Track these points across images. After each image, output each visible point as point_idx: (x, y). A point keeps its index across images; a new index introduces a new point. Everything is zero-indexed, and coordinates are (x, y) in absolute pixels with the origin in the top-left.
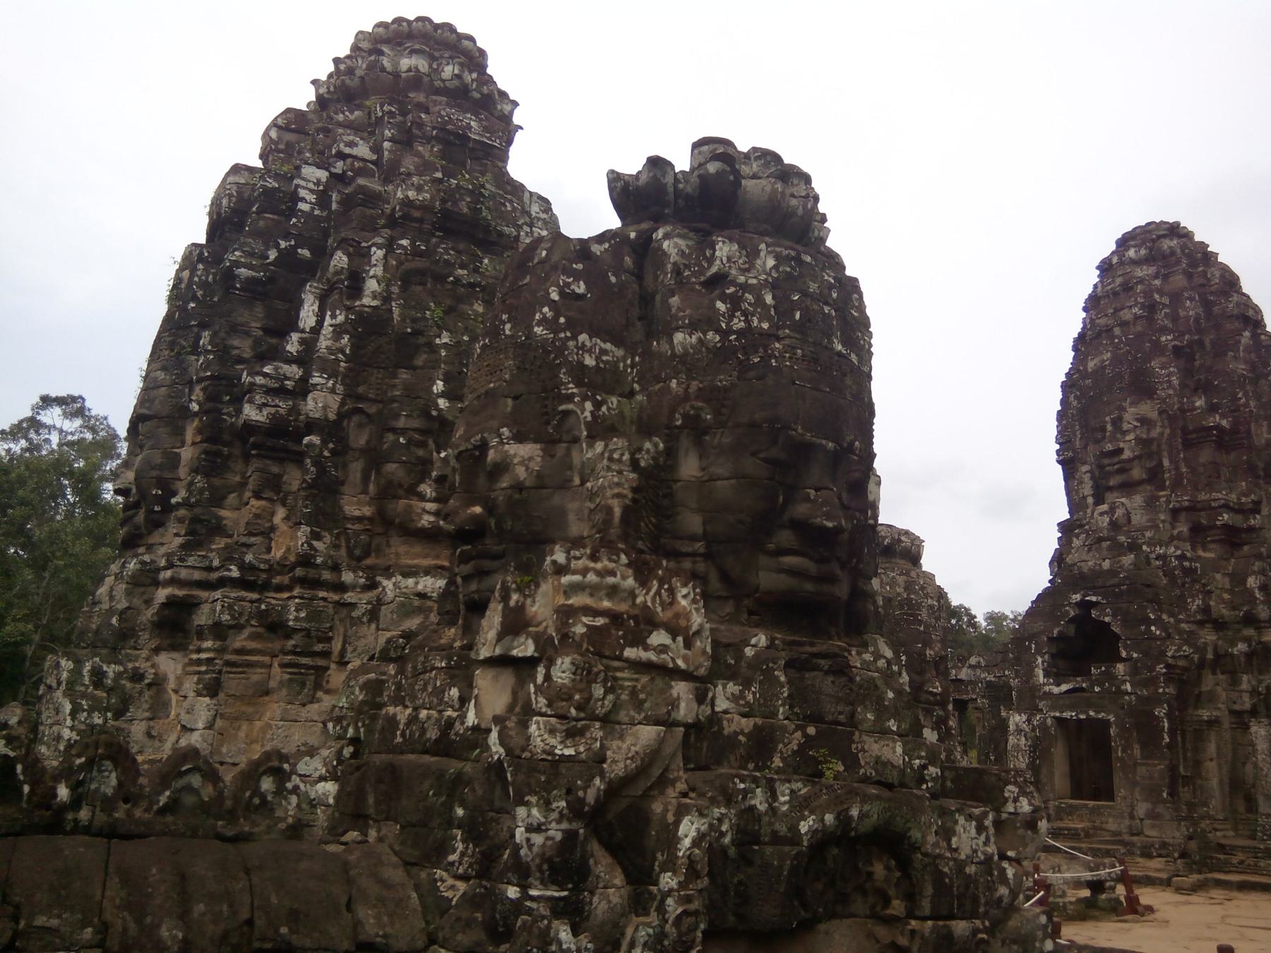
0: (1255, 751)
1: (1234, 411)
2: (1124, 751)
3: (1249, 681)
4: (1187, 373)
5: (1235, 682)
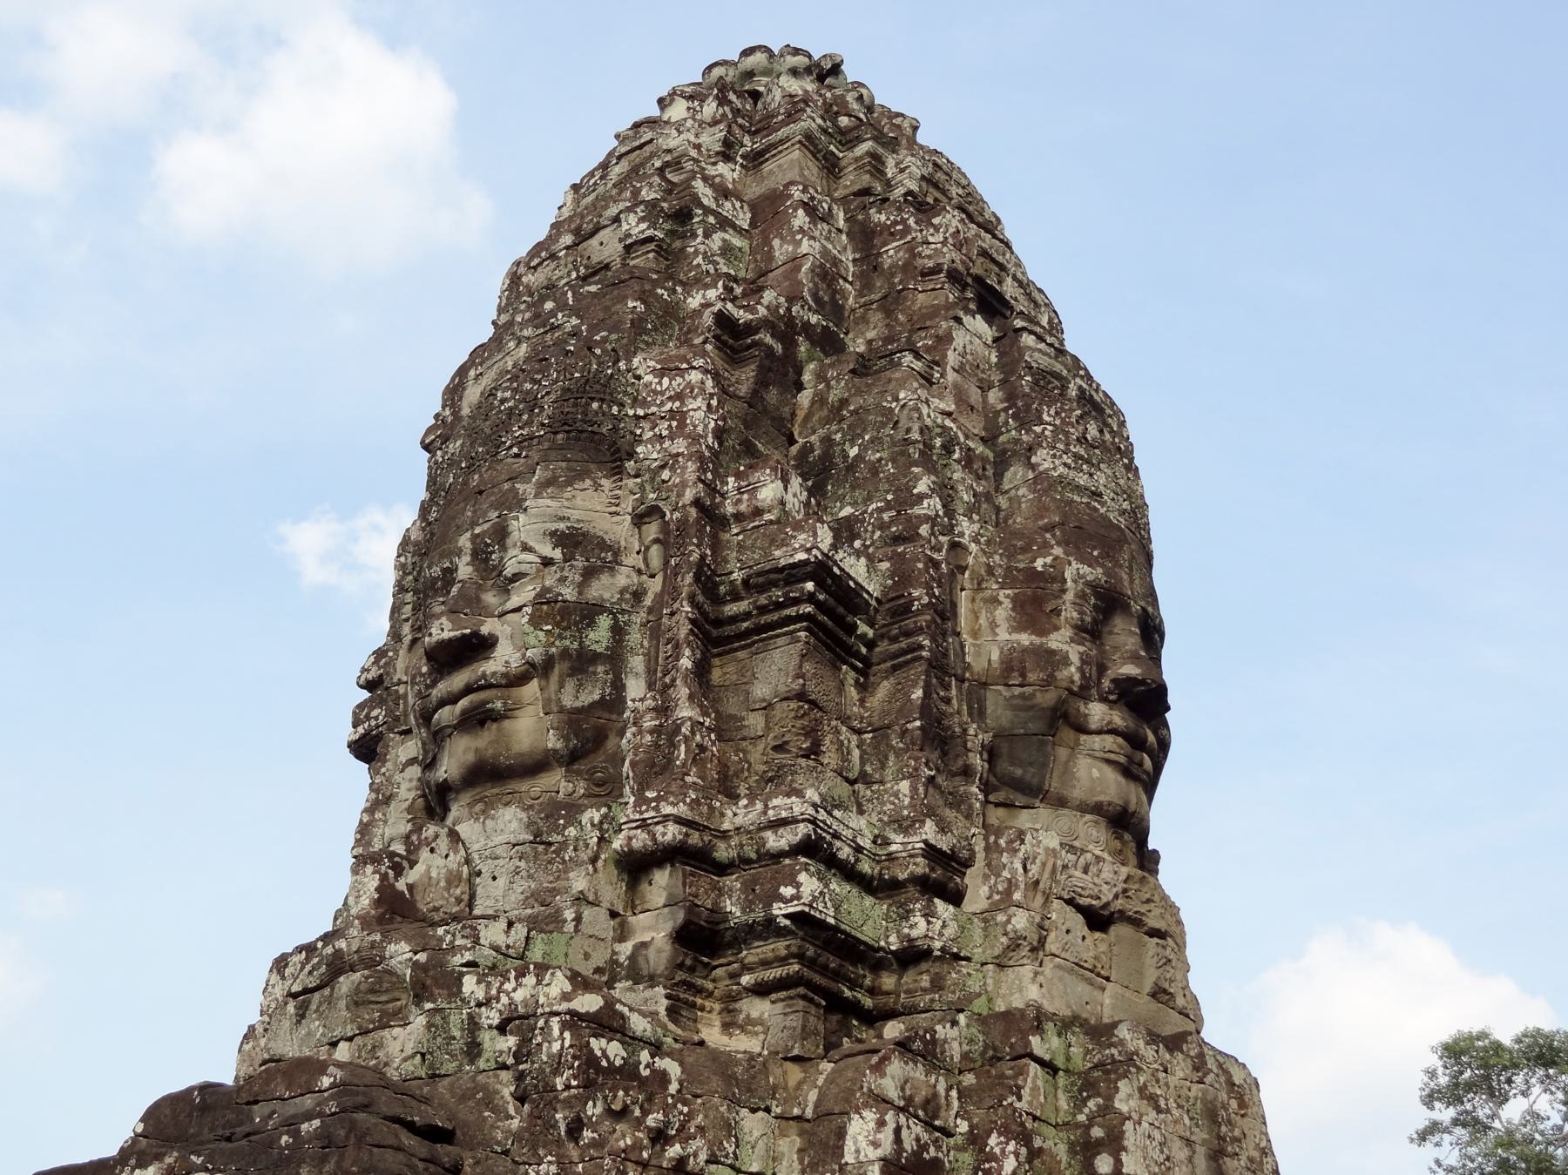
1: (897, 539)
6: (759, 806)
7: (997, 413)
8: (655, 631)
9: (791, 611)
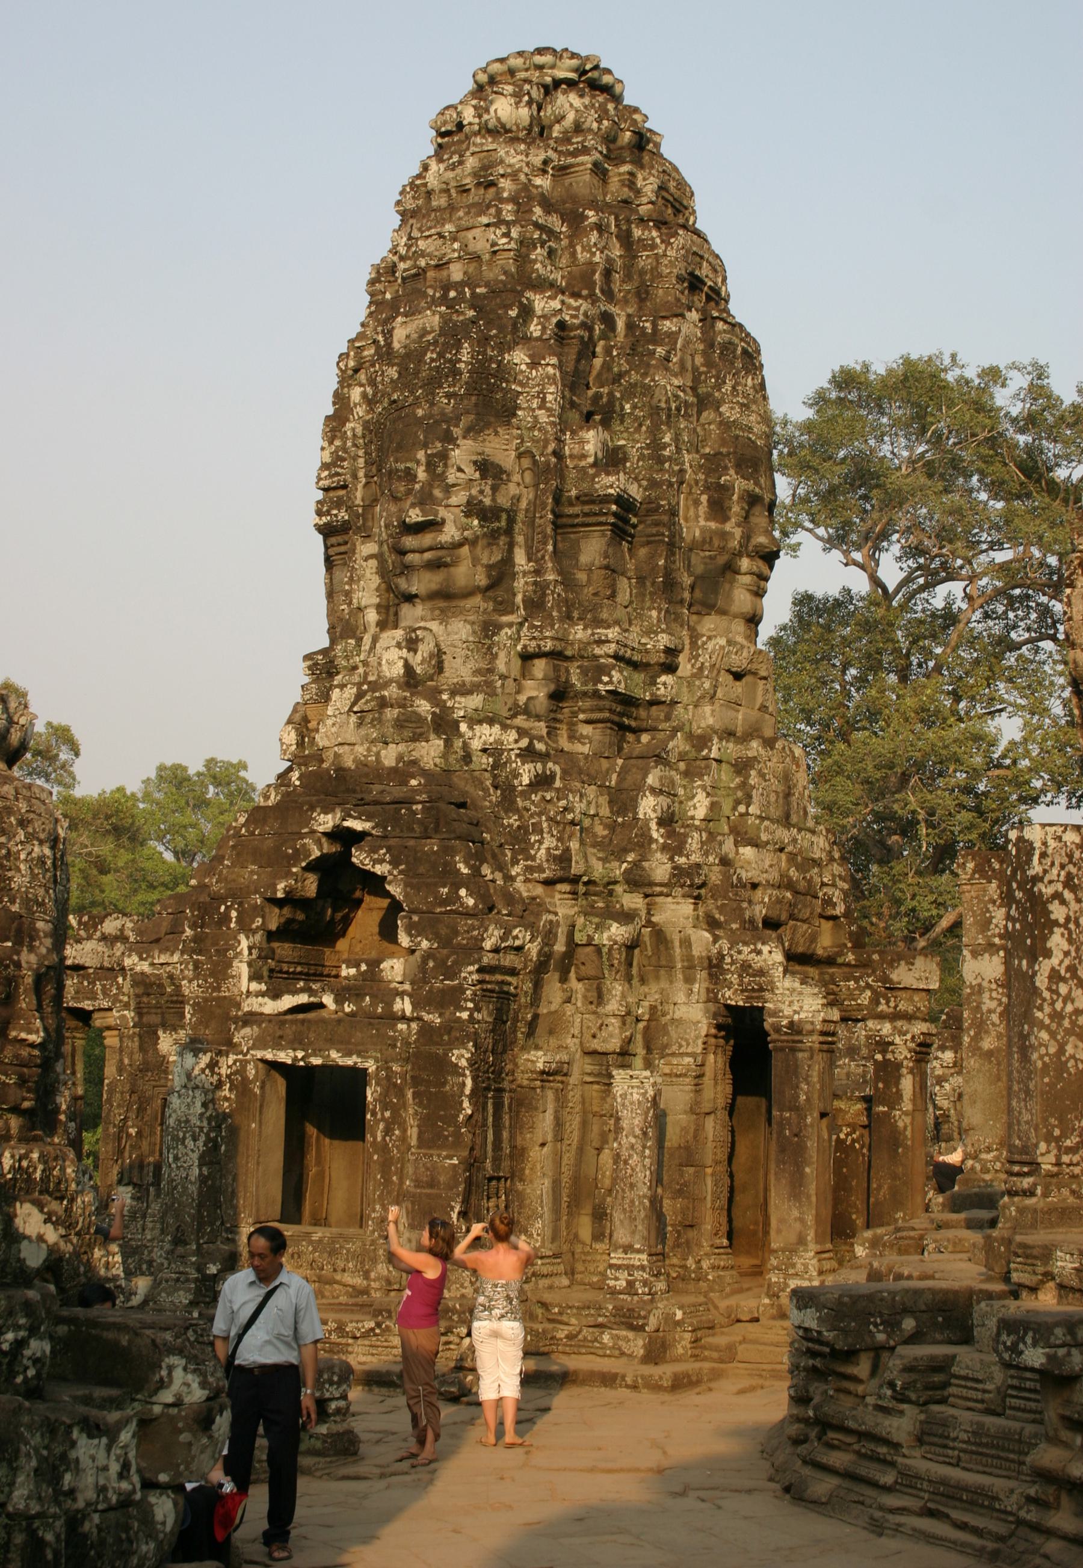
0: (618, 1129)
2: (388, 1131)
3: (624, 996)
4: (574, 382)
5: (600, 998)
6: (589, 631)
7: (700, 374)
8: (531, 523)
9: (603, 519)
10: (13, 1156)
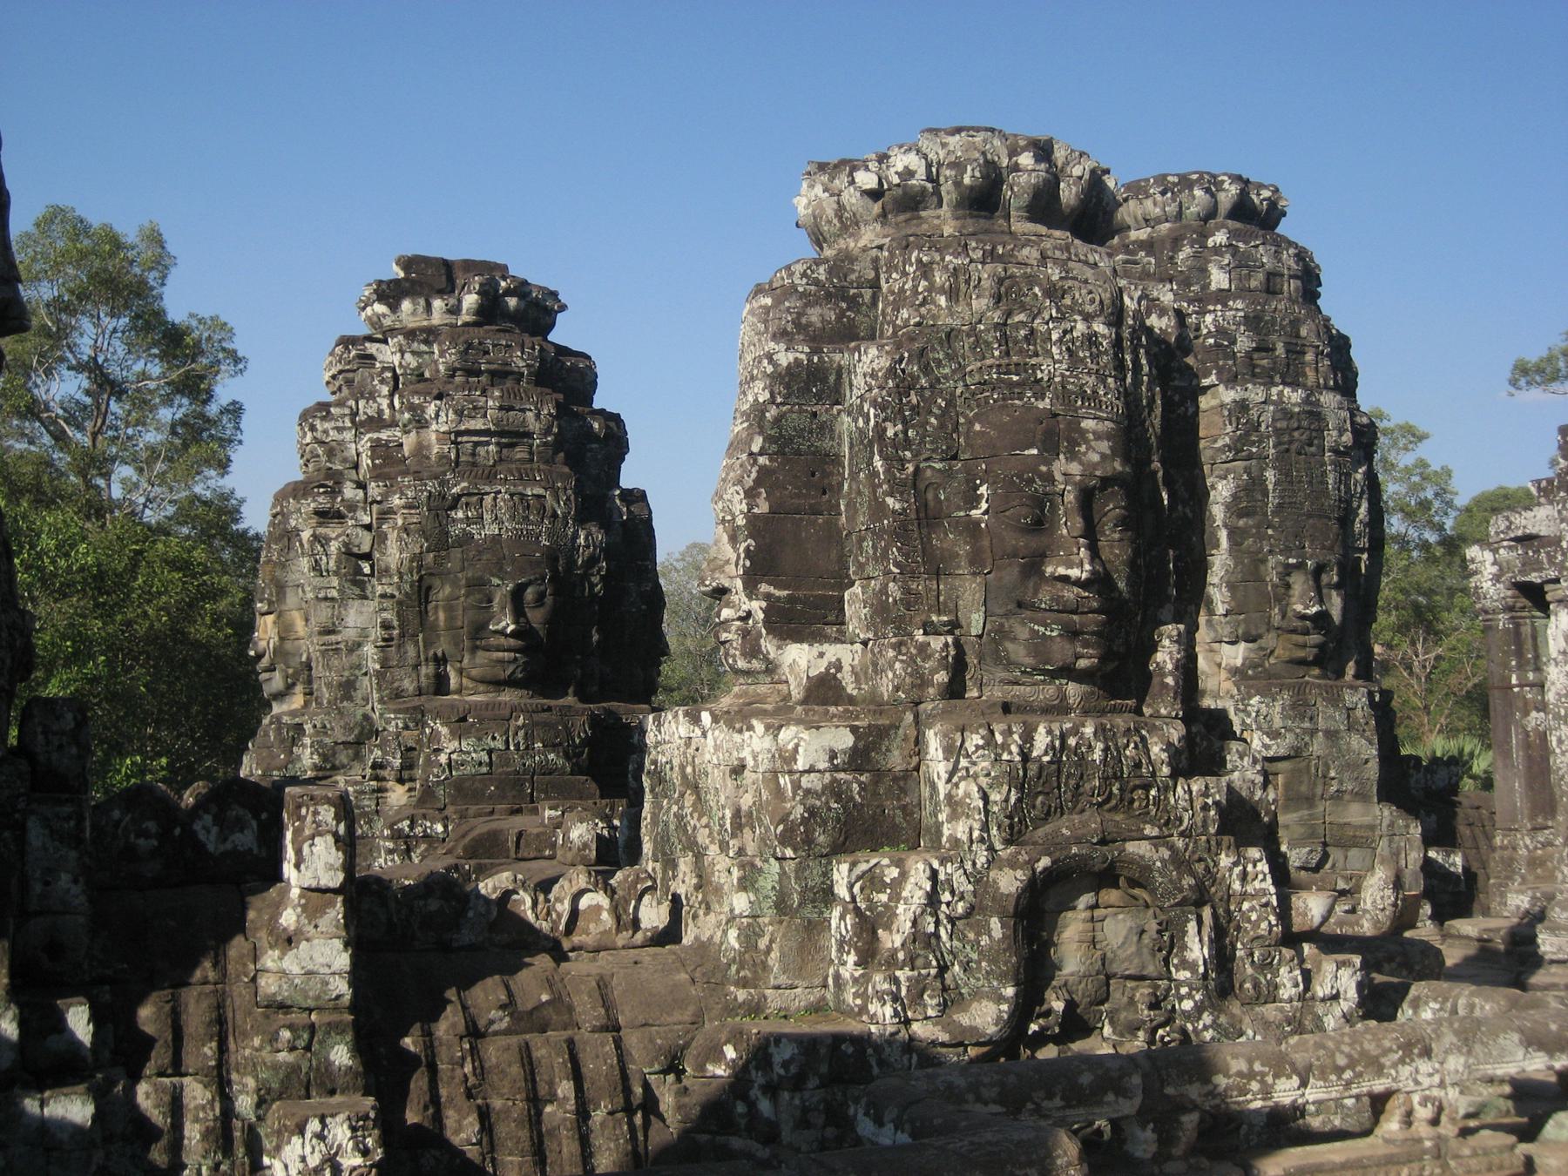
10: (1050, 732)
